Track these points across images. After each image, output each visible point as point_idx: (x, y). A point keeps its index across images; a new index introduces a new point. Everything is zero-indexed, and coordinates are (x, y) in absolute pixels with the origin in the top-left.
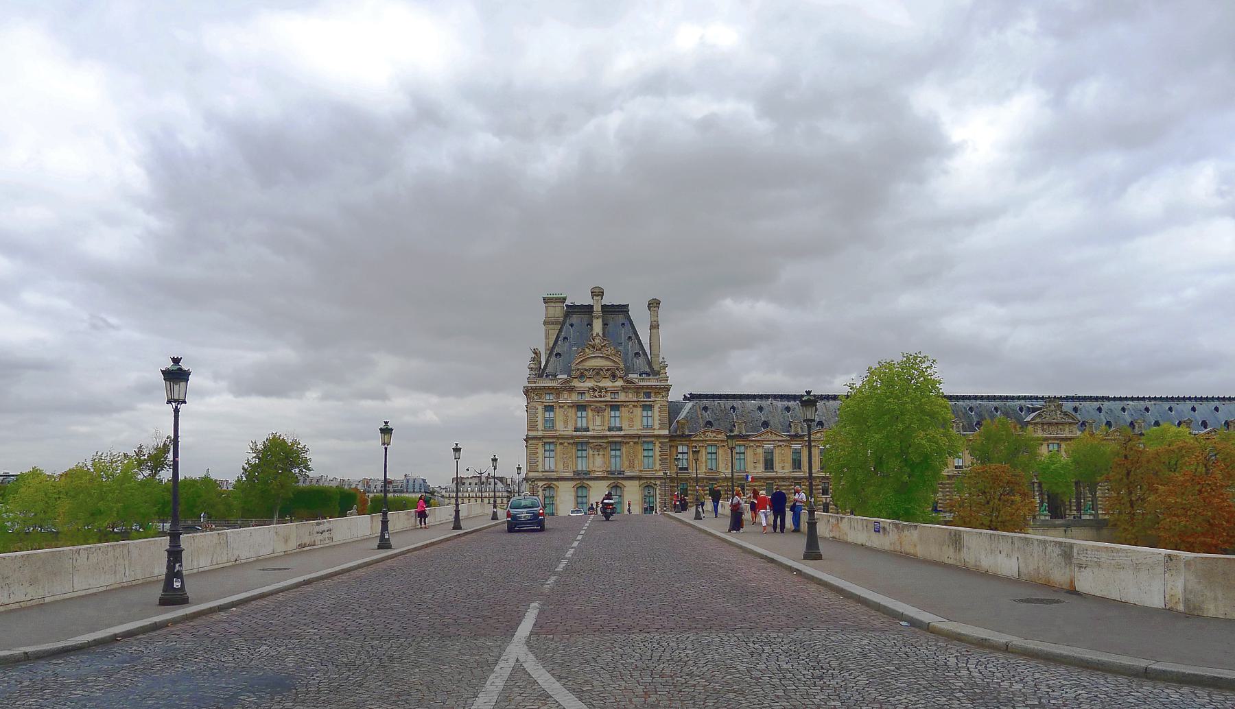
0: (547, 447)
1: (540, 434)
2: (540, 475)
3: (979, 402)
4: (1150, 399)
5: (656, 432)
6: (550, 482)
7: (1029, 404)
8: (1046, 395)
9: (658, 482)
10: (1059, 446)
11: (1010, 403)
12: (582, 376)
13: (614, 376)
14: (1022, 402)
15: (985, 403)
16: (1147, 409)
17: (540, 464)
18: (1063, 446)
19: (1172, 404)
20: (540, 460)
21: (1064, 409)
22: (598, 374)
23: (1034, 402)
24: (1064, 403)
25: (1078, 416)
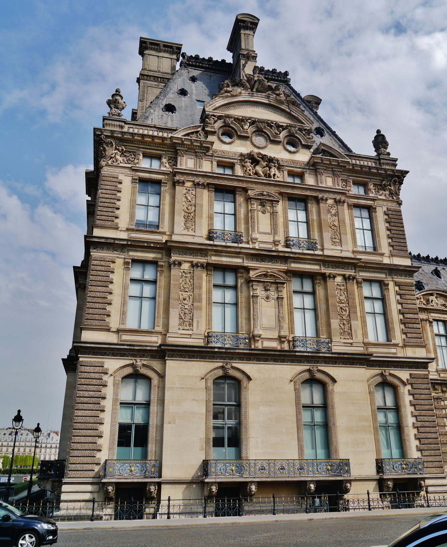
2: (112, 338)
6: (149, 358)
9: (404, 374)
12: (229, 132)
13: (293, 141)
17: (114, 310)
20: (116, 299)
22: (259, 132)
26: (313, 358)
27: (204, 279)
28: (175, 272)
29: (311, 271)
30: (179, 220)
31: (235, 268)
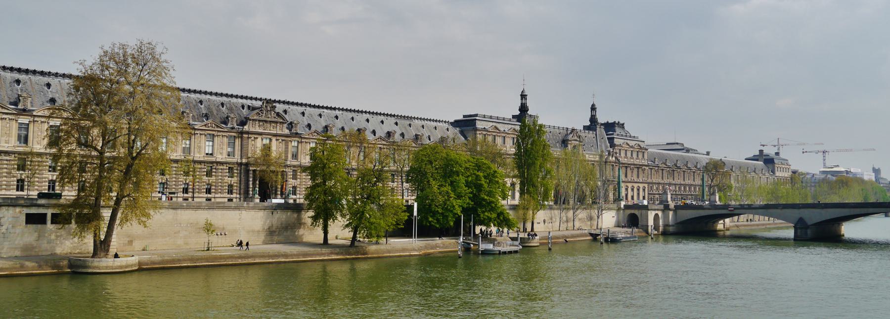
3: (208, 96)
4: (339, 109)
7: (249, 102)
8: (264, 97)
10: (271, 140)
11: (234, 100)
14: (244, 101)
15: (214, 98)
18: (274, 139)
21: (277, 110)
23: (254, 102)
24: (277, 105)
25: (286, 117)
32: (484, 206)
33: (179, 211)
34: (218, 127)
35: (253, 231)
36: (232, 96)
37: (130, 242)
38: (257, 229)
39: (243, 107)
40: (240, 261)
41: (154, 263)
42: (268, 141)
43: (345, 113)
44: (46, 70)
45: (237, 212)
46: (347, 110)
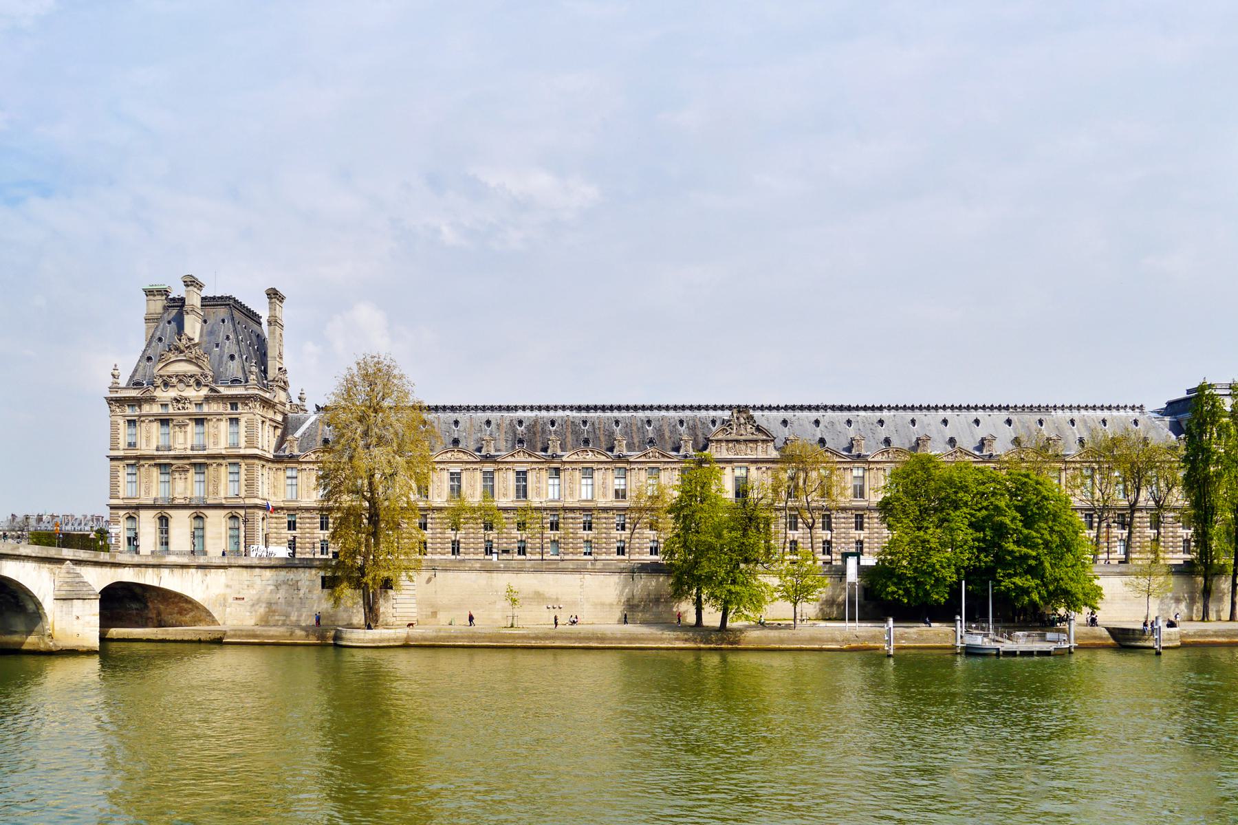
0: (130, 470)
1: (121, 453)
4: (889, 408)
5: (242, 452)
9: (242, 512)
10: (748, 469)
16: (881, 422)
17: (121, 489)
19: (917, 415)
20: (121, 484)
26: (197, 507)
27: (155, 472)
28: (142, 469)
29: (200, 463)
30: (144, 441)
31: (166, 465)
32: (1010, 565)
33: (495, 575)
34: (663, 456)
35: (603, 604)
36: (699, 408)
37: (434, 614)
38: (608, 601)
39: (714, 422)
40: (533, 643)
41: (426, 640)
42: (744, 471)
43: (901, 413)
44: (456, 404)
45: (577, 576)
46: (905, 408)
